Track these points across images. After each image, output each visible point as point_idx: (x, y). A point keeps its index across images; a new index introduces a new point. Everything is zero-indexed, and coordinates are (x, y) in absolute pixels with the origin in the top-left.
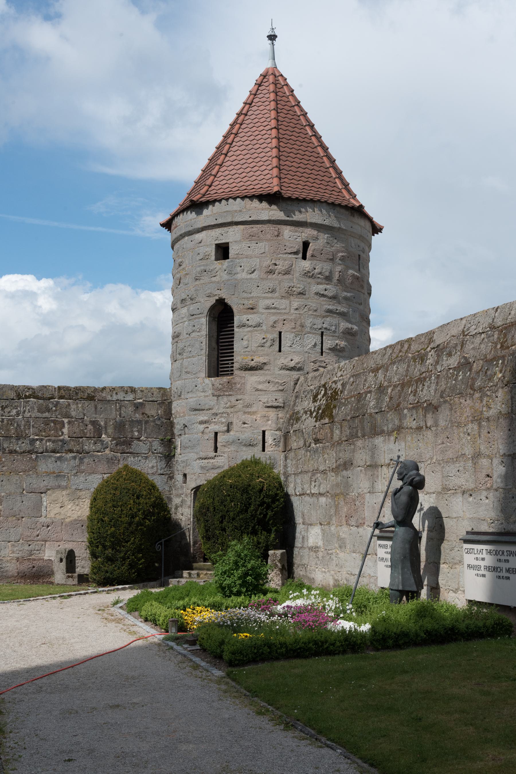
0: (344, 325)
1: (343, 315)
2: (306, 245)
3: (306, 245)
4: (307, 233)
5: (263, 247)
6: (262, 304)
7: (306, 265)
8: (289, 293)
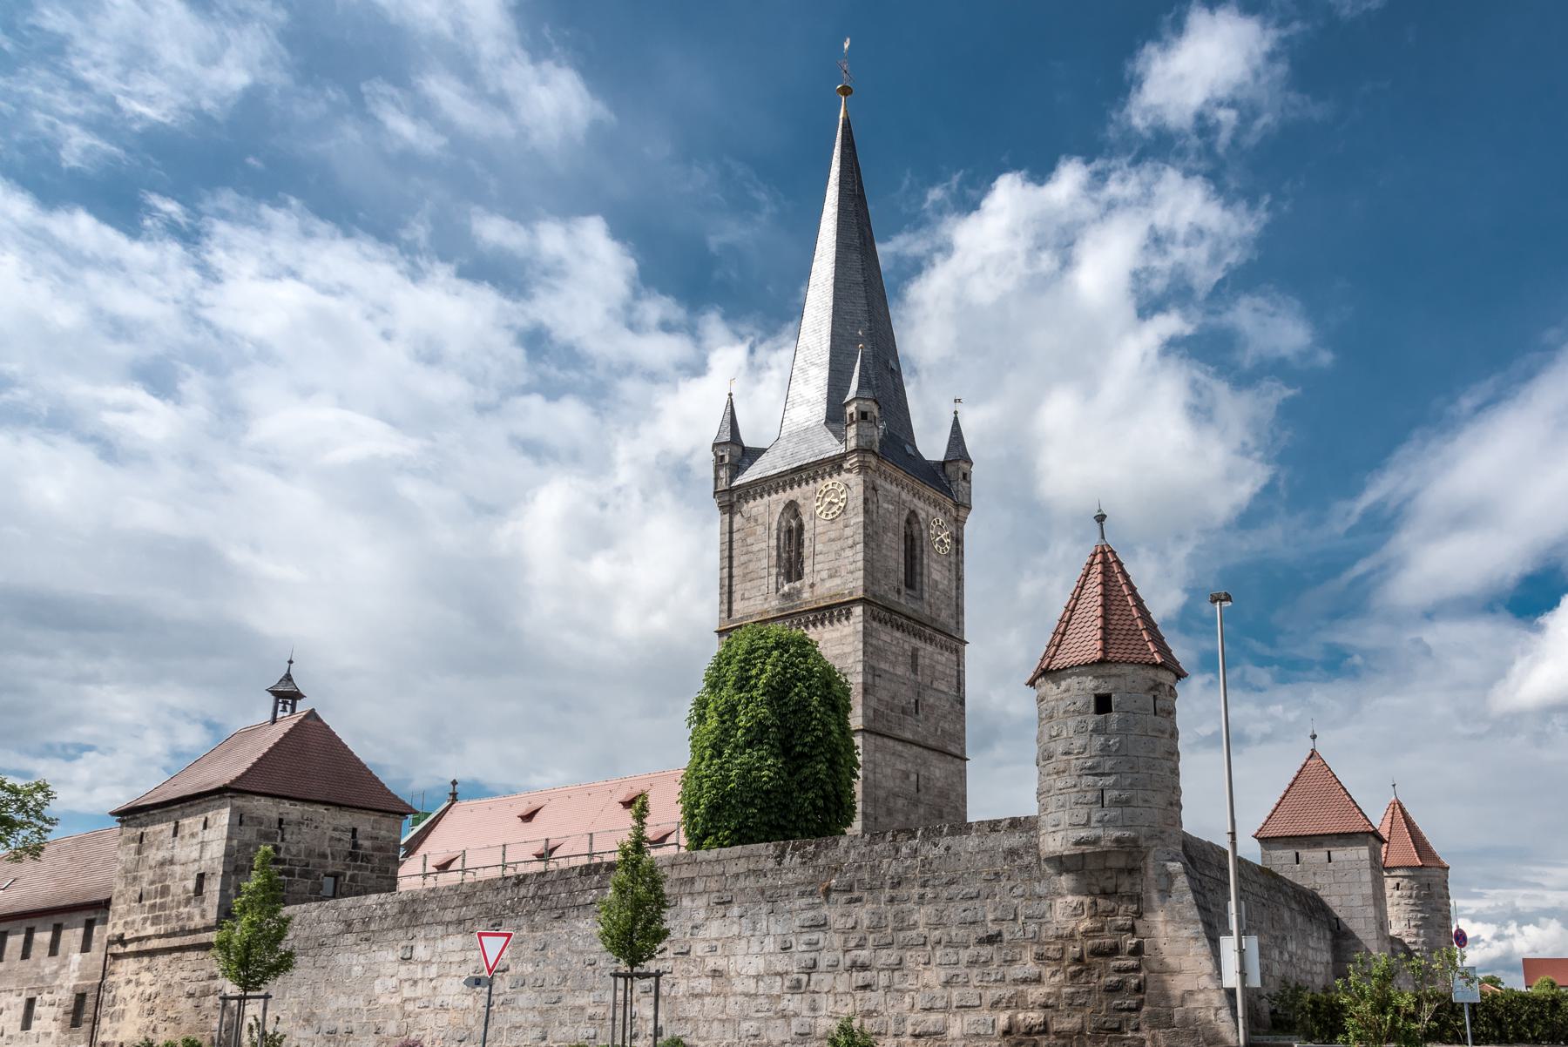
0: (1420, 915)
1: (1419, 911)
2: (1398, 884)
3: (1398, 884)
4: (1398, 880)
7: (1399, 893)
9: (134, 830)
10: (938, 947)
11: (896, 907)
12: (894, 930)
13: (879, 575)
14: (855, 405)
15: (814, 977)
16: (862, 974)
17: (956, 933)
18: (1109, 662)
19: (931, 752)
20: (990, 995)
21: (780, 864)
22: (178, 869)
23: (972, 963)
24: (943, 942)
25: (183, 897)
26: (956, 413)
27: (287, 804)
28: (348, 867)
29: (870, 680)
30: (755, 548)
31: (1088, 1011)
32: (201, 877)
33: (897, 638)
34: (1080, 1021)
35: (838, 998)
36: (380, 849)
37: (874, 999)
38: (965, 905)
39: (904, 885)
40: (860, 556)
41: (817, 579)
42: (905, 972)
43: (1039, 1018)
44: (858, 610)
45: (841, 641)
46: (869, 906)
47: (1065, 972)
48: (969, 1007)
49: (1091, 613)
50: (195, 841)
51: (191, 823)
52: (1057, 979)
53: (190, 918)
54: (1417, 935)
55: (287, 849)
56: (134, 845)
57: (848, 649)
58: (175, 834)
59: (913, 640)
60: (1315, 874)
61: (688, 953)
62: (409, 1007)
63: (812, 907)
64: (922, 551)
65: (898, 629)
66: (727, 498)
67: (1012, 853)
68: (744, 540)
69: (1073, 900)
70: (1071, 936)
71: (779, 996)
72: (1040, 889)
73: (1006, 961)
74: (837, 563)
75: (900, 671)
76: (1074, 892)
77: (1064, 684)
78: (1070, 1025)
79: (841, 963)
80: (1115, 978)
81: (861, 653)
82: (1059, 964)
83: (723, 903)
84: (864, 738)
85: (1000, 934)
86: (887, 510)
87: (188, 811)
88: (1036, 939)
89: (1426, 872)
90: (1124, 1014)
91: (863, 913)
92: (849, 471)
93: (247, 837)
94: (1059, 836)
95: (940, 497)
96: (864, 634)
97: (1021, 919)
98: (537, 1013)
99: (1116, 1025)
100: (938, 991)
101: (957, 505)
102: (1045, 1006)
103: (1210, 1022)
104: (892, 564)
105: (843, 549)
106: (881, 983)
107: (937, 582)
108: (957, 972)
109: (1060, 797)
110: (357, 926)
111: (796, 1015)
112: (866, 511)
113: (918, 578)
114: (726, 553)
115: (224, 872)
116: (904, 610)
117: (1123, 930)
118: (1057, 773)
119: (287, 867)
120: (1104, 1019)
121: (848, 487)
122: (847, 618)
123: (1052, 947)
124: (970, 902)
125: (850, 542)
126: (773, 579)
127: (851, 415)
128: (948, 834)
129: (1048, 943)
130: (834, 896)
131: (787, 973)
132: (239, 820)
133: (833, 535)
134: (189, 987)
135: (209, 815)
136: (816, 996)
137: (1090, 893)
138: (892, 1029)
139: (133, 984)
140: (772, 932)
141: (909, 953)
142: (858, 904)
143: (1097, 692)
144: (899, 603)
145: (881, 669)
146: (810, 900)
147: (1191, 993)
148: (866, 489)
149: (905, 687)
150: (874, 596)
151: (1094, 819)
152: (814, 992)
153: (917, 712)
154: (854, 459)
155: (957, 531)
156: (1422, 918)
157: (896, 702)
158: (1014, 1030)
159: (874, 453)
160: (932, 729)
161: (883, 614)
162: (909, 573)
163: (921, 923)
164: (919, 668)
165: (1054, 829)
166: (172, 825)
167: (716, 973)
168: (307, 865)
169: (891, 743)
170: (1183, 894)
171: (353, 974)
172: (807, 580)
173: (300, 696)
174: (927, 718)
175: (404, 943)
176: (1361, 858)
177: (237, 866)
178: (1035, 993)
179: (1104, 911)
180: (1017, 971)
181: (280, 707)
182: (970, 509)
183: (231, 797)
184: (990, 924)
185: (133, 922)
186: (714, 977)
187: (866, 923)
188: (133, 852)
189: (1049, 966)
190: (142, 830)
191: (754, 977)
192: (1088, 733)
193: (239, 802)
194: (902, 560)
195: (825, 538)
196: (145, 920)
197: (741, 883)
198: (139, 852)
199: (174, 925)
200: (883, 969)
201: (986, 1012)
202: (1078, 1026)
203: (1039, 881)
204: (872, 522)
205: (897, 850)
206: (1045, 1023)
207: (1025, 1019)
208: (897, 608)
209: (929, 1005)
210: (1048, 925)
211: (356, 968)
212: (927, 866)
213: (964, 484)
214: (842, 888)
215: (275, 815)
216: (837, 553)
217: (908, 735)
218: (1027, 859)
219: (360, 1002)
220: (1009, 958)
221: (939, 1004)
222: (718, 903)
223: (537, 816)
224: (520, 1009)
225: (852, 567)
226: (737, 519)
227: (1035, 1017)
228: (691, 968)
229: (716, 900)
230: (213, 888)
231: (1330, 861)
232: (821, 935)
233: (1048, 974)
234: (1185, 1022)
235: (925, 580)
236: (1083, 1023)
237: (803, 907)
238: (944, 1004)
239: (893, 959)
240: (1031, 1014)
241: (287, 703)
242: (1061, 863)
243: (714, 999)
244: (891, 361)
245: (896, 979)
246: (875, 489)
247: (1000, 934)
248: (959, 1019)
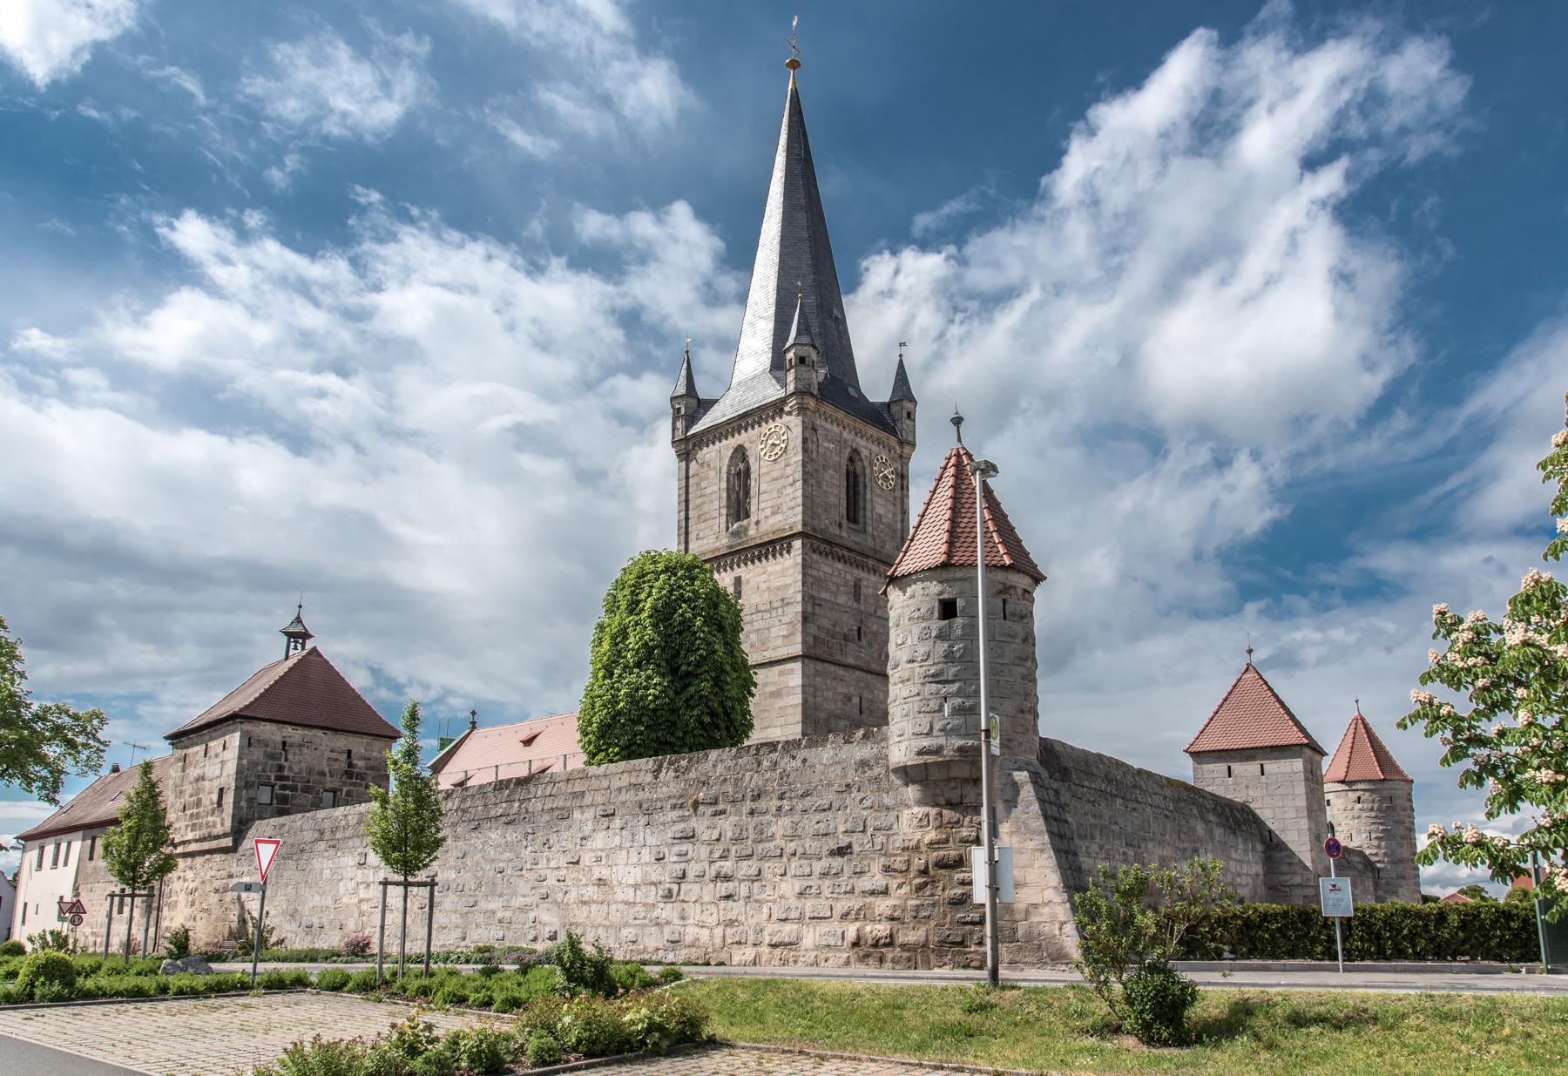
0: (1381, 827)
1: (1381, 824)
2: (1359, 798)
3: (1359, 798)
4: (1359, 793)
5: (1340, 801)
6: (1343, 823)
7: (1360, 806)
8: (1353, 818)
9: (180, 751)
10: (794, 859)
11: (756, 819)
12: (753, 841)
13: (819, 510)
14: (793, 351)
15: (683, 886)
16: (725, 885)
17: (809, 844)
18: (954, 565)
19: (874, 677)
20: (841, 907)
21: (656, 778)
22: (207, 784)
23: (825, 875)
24: (798, 854)
25: (210, 808)
26: (901, 356)
27: (289, 728)
28: (345, 784)
29: (809, 609)
30: (708, 491)
31: (933, 923)
32: (221, 790)
33: (838, 569)
34: (924, 934)
35: (704, 908)
36: (372, 768)
37: (735, 909)
38: (818, 817)
39: (763, 797)
40: (800, 493)
41: (761, 517)
42: (764, 883)
43: (885, 930)
44: (797, 544)
45: (783, 574)
46: (733, 819)
47: (910, 883)
48: (821, 918)
49: (940, 517)
50: (218, 760)
51: (216, 745)
52: (903, 891)
53: (214, 826)
54: (1379, 847)
55: (290, 768)
56: (181, 764)
57: (789, 581)
58: (205, 756)
59: (856, 571)
60: (1247, 787)
61: (577, 863)
62: (364, 907)
63: (683, 819)
64: (865, 486)
65: (839, 561)
66: (683, 447)
67: (863, 764)
68: (698, 484)
69: (919, 811)
70: (917, 848)
71: (654, 905)
72: (888, 800)
73: (855, 873)
74: (779, 501)
75: (842, 600)
76: (921, 803)
77: (909, 590)
78: (915, 938)
79: (707, 873)
80: (959, 891)
81: (800, 584)
82: (905, 877)
83: (607, 816)
84: (803, 663)
85: (850, 846)
86: (828, 449)
87: (214, 735)
88: (883, 851)
89: (1388, 785)
90: (968, 927)
91: (727, 825)
92: (789, 413)
93: (255, 757)
94: (903, 746)
95: (883, 435)
96: (804, 566)
97: (870, 831)
98: (458, 916)
99: (959, 939)
100: (793, 902)
101: (901, 443)
102: (892, 919)
103: (1054, 936)
104: (833, 500)
105: (785, 487)
106: (742, 893)
107: (880, 515)
108: (810, 883)
109: (905, 706)
110: (327, 835)
111: (668, 923)
112: (805, 450)
113: (861, 513)
114: (683, 498)
115: (236, 787)
116: (847, 544)
117: (967, 842)
118: (903, 682)
119: (290, 783)
120: (948, 933)
121: (790, 427)
122: (788, 552)
123: (899, 859)
124: (823, 814)
125: (791, 480)
126: (723, 519)
127: (790, 360)
128: (805, 747)
129: (895, 855)
130: (701, 808)
131: (660, 883)
132: (248, 742)
133: (775, 474)
134: (217, 884)
135: (227, 738)
136: (685, 905)
137: (936, 805)
138: (751, 939)
139: (181, 881)
140: (648, 844)
141: (767, 865)
142: (722, 816)
143: (942, 597)
144: (841, 537)
145: (820, 599)
146: (681, 813)
147: (1035, 906)
148: (804, 429)
149: (847, 615)
150: (814, 529)
151: (937, 727)
152: (683, 901)
153: (859, 639)
154: (793, 402)
155: (902, 467)
156: (1383, 831)
157: (837, 629)
158: (862, 942)
159: (812, 395)
160: (876, 655)
161: (823, 547)
162: (852, 508)
163: (778, 835)
164: (862, 597)
165: (899, 739)
166: (204, 746)
167: (601, 882)
168: (308, 782)
169: (832, 668)
170: (1029, 804)
171: (324, 878)
172: (753, 519)
173: (310, 636)
174: (870, 645)
175: (360, 850)
176: (1295, 770)
177: (247, 783)
178: (883, 905)
179: (949, 823)
180: (865, 883)
181: (292, 645)
182: (914, 445)
183: (241, 723)
184: (841, 836)
185: (180, 828)
186: (599, 885)
187: (729, 834)
188: (179, 770)
189: (895, 878)
190: (185, 751)
191: (632, 886)
192: (932, 640)
193: (248, 727)
194: (843, 496)
195: (768, 478)
196: (187, 826)
197: (623, 797)
198: (183, 770)
199: (204, 832)
200: (744, 880)
201: (836, 923)
202: (923, 939)
203: (887, 793)
204: (812, 460)
205: (759, 764)
206: (891, 936)
207: (871, 932)
208: (839, 541)
209: (784, 917)
210: (895, 837)
211: (326, 872)
212: (785, 779)
213: (908, 422)
214: (709, 801)
215: (279, 739)
216: (780, 491)
217: (851, 661)
218: (877, 770)
219: (329, 902)
220: (858, 870)
221: (794, 914)
222: (603, 816)
223: (536, 741)
224: (447, 912)
225: (791, 504)
226: (693, 465)
227: (882, 929)
228: (581, 877)
229: (601, 813)
230: (229, 799)
231: (1263, 774)
232: (690, 847)
233: (895, 886)
234: (1029, 937)
235: (869, 514)
236: (927, 936)
237: (675, 819)
238: (797, 915)
239: (753, 871)
240: (878, 926)
241: (298, 642)
242: (907, 774)
243: (599, 906)
244: (835, 311)
245: (755, 891)
246: (814, 429)
247: (850, 846)
248: (812, 930)
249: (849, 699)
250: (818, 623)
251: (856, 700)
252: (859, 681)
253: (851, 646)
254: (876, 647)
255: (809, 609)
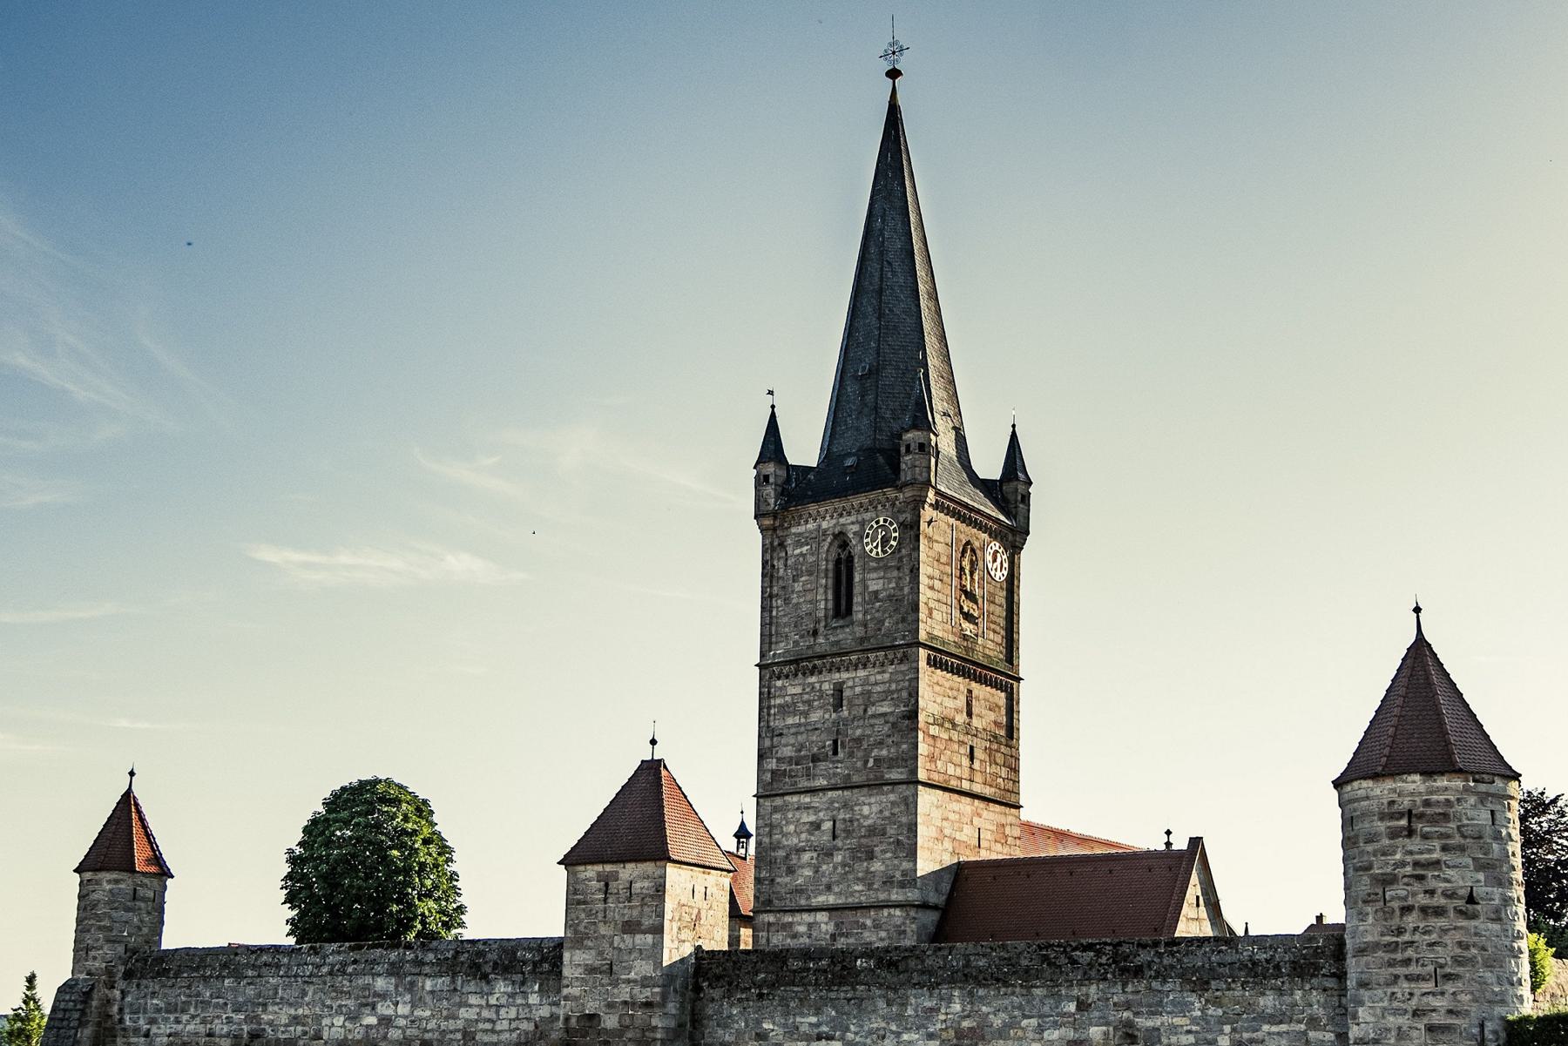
75: (815, 717)
153: (835, 753)
160: (859, 764)
174: (851, 755)
249: (816, 826)
250: (779, 755)
251: (827, 825)
252: (832, 802)
253: (822, 765)
254: (860, 754)
255: (767, 743)
